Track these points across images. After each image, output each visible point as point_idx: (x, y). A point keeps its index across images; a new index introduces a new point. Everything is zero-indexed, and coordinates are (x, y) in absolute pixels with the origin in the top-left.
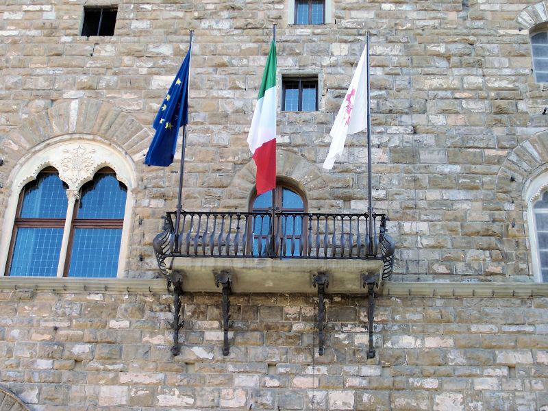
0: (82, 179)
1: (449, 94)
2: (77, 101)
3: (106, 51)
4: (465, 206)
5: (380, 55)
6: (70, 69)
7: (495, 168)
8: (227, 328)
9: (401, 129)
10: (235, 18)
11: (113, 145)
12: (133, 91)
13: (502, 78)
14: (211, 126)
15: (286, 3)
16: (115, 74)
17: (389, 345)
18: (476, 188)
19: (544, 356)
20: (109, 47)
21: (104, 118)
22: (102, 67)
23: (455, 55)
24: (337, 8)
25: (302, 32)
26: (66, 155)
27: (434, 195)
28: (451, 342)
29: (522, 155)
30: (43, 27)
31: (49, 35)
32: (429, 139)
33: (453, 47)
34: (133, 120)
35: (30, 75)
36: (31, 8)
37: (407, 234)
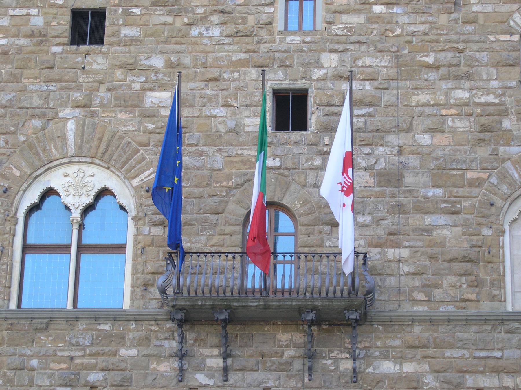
0: (84, 205)
1: (435, 110)
2: (73, 121)
3: (98, 64)
4: (446, 232)
5: (370, 66)
6: (63, 84)
7: (475, 191)
8: (226, 356)
9: (388, 150)
10: (225, 23)
11: (112, 169)
12: (127, 109)
13: (488, 92)
14: (206, 149)
15: (275, 5)
16: (109, 90)
17: (371, 370)
18: (457, 213)
19: (509, 380)
20: (100, 59)
21: (101, 139)
22: (94, 82)
23: (444, 66)
24: (328, 11)
25: (293, 40)
26: (67, 179)
27: (415, 220)
28: (426, 367)
29: (503, 176)
30: (31, 35)
31: (39, 44)
32: (413, 161)
33: (442, 55)
34: (129, 142)
35: (25, 91)
36: (17, 12)
37: (390, 261)
